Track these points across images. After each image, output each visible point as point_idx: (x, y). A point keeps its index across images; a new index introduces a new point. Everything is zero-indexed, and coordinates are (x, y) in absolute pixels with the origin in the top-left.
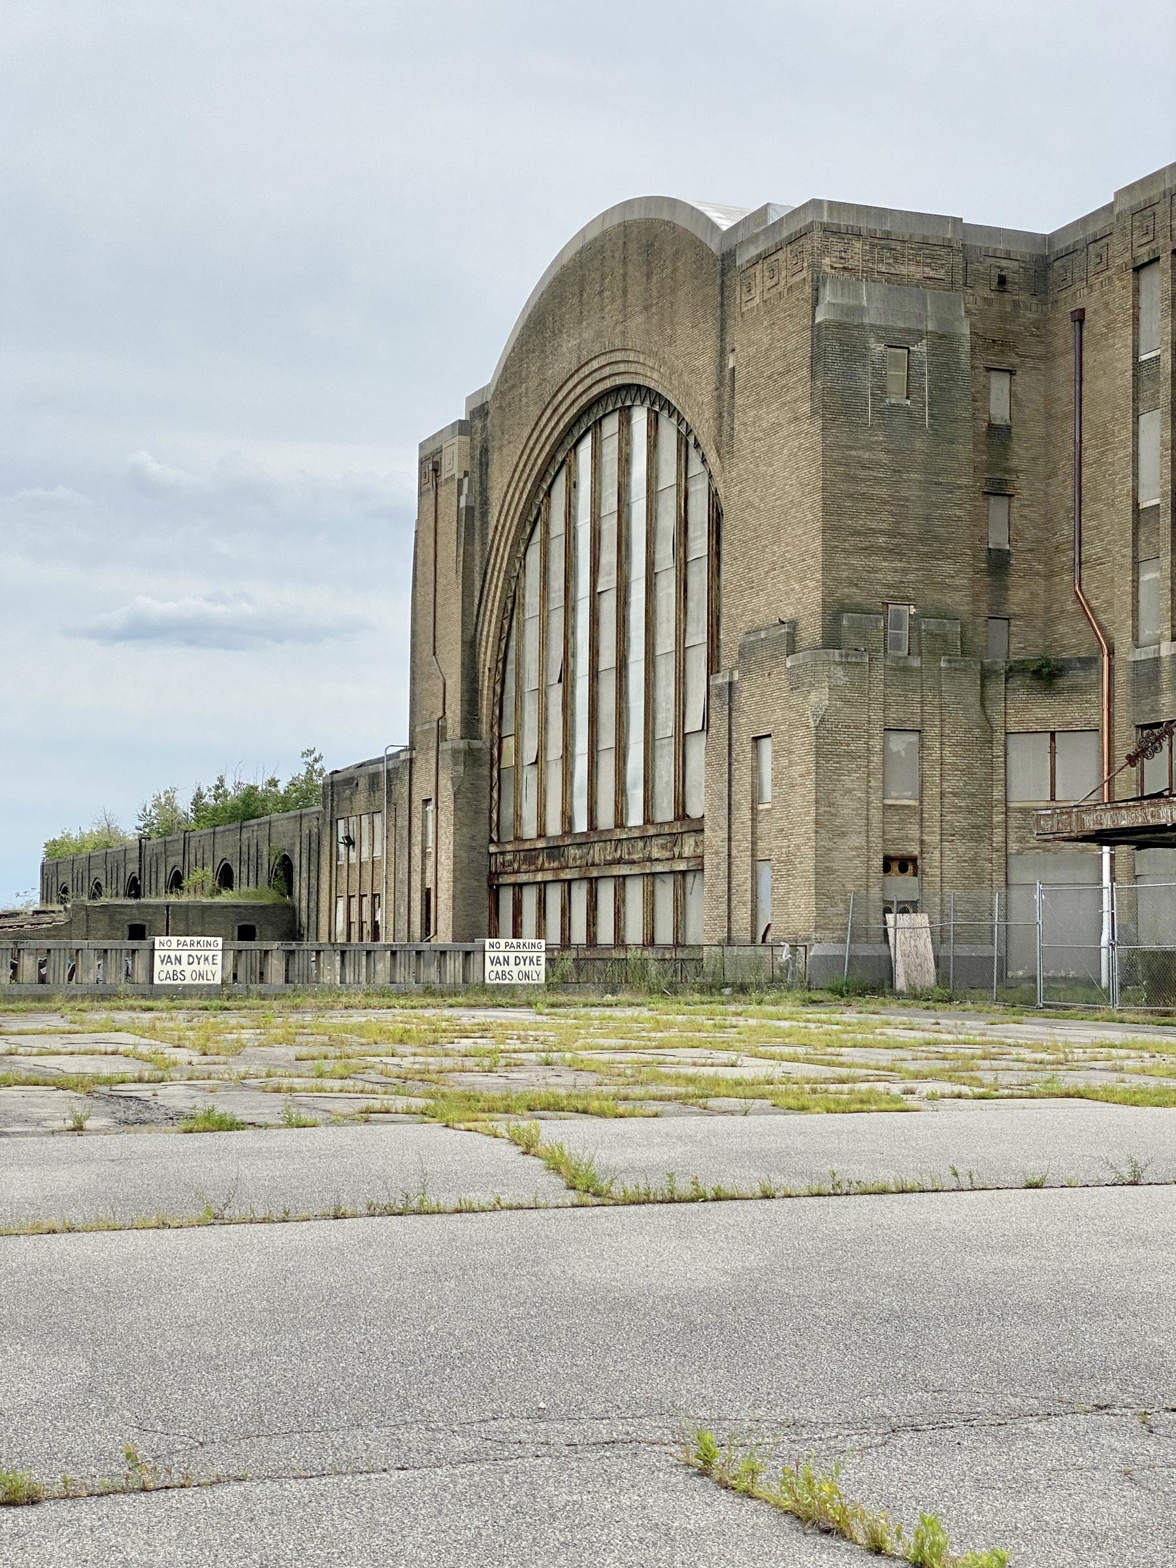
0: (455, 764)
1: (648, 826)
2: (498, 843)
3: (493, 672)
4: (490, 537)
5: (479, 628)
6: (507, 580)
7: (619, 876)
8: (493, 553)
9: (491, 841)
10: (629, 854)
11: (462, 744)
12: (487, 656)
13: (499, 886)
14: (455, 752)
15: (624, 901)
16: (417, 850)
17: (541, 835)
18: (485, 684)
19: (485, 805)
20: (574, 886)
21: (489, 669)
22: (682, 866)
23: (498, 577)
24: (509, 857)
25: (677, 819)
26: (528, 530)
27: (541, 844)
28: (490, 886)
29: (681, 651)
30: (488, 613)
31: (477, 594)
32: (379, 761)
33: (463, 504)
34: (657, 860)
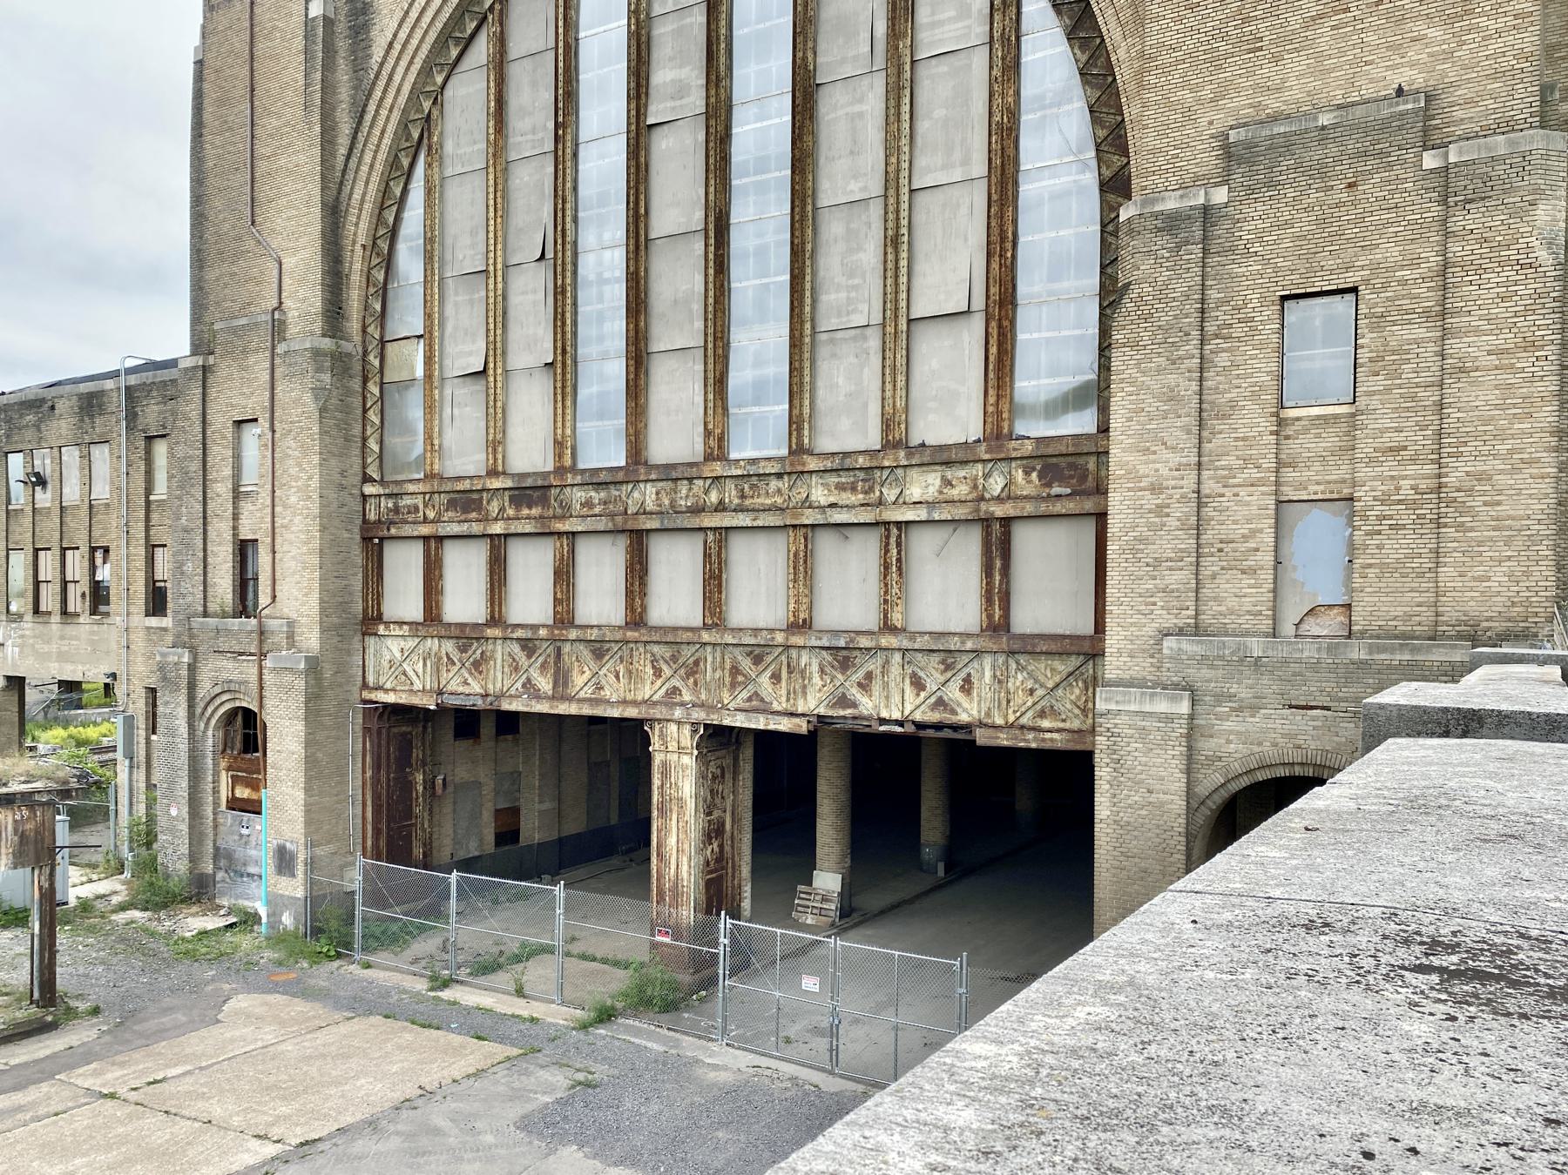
0: (319, 370)
2: (382, 482)
4: (377, 57)
7: (715, 529)
8: (381, 83)
9: (367, 479)
10: (743, 497)
11: (327, 344)
12: (358, 228)
13: (382, 539)
14: (317, 353)
16: (221, 490)
18: (356, 265)
19: (357, 430)
21: (364, 246)
22: (910, 515)
23: (388, 118)
25: (889, 445)
26: (454, 53)
27: (496, 484)
29: (898, 192)
30: (365, 168)
32: (115, 375)
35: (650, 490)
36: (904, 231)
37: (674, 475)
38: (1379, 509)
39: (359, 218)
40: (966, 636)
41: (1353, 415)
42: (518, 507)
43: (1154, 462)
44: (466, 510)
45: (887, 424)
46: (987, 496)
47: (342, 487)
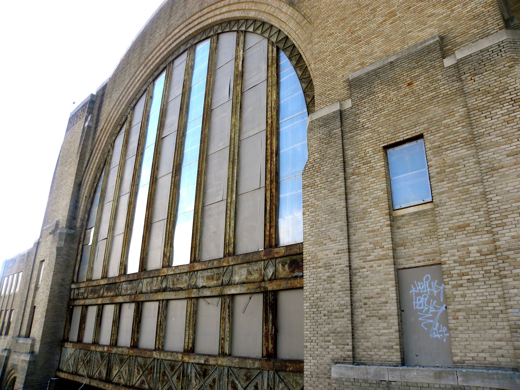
1: (196, 264)
3: (87, 199)
5: (84, 178)
6: (103, 154)
7: (163, 300)
10: (174, 285)
12: (85, 191)
15: (166, 317)
17: (105, 276)
20: (126, 307)
21: (86, 197)
24: (82, 291)
27: (103, 282)
28: (69, 306)
31: (86, 162)
33: (87, 124)
34: (204, 287)
35: (145, 281)
36: (236, 157)
37: (152, 275)
38: (458, 269)
39: (86, 187)
40: (255, 359)
41: (433, 209)
42: (108, 292)
43: (325, 250)
44: (95, 294)
45: (226, 245)
46: (266, 279)
47: (61, 285)
